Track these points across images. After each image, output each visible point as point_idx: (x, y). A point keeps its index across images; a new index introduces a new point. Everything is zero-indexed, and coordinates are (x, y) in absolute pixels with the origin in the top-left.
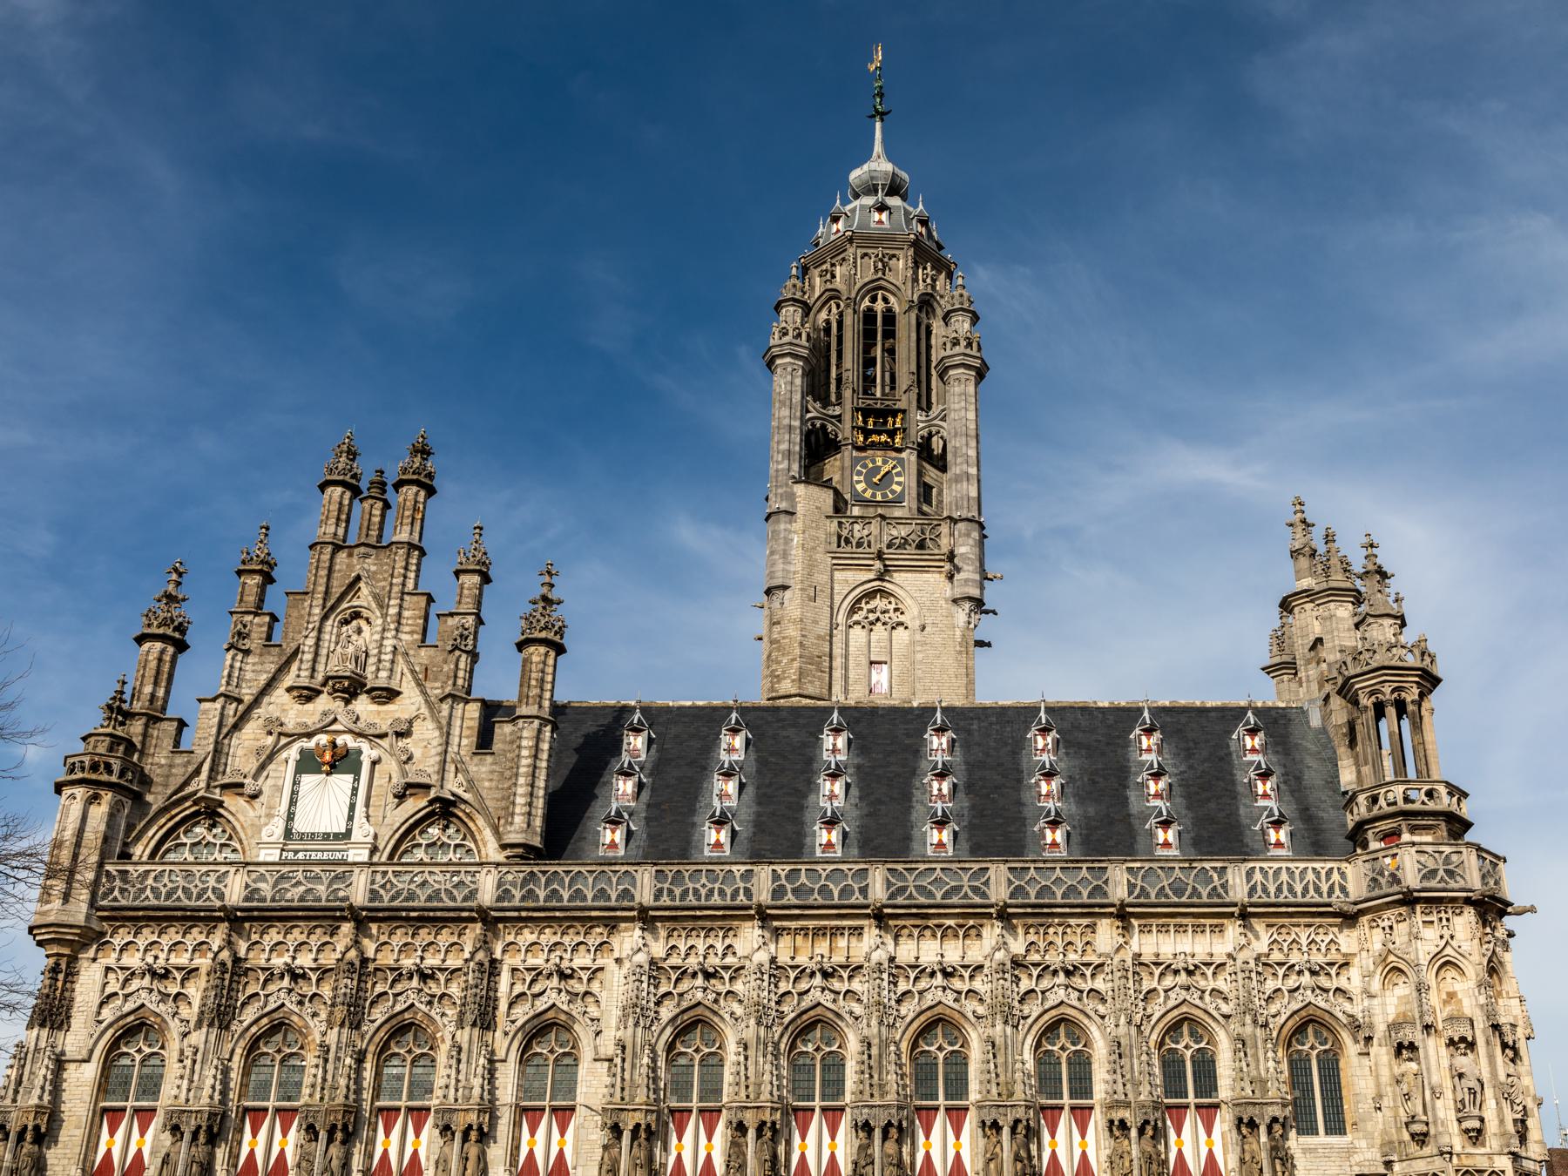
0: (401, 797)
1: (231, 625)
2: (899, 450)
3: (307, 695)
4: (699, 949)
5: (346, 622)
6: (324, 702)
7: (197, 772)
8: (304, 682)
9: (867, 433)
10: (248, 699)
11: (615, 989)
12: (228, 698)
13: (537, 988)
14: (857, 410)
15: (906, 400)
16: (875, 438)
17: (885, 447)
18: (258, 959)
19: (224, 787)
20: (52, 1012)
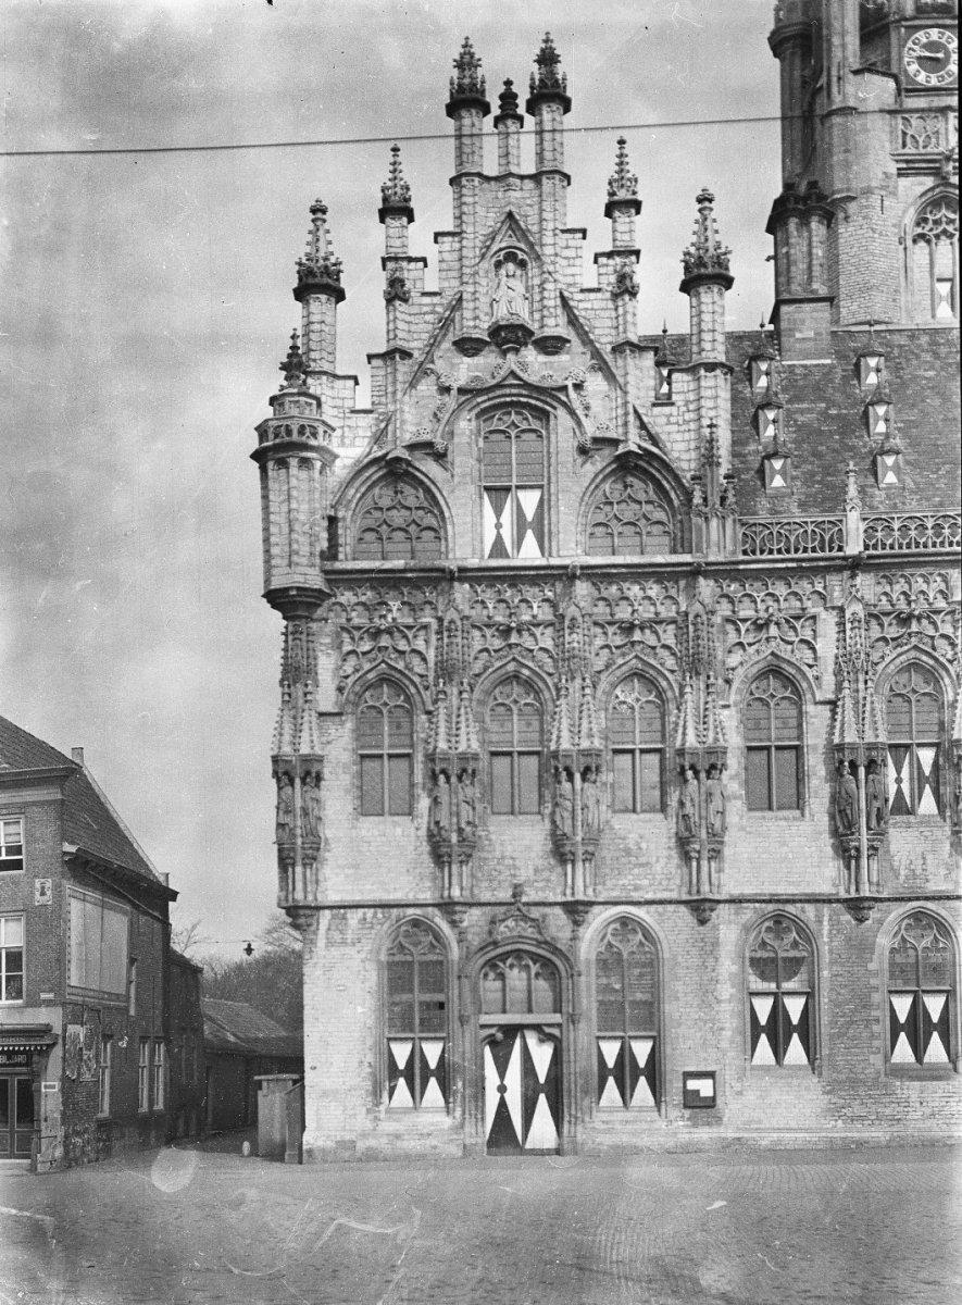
5: (498, 265)
19: (412, 447)
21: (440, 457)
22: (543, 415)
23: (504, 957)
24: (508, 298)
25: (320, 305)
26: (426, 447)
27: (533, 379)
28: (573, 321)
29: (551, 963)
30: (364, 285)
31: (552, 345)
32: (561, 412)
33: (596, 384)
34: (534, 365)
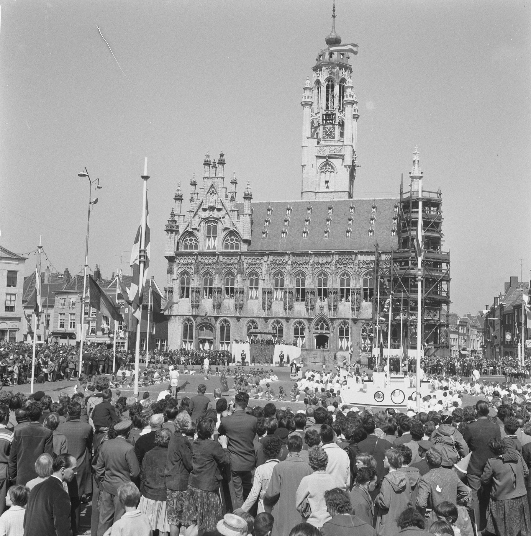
0: (224, 230)
1: (191, 196)
2: (334, 125)
3: (205, 210)
4: (279, 259)
5: (211, 194)
6: (208, 211)
7: (188, 226)
8: (204, 207)
9: (326, 120)
10: (195, 211)
11: (264, 268)
12: (192, 212)
13: (251, 266)
14: (323, 115)
15: (336, 112)
16: (328, 122)
17: (331, 124)
18: (202, 261)
19: (193, 229)
20: (170, 272)
21: (198, 231)
22: (217, 223)
23: (204, 326)
24: (211, 201)
25: (178, 202)
26: (196, 229)
27: (215, 216)
28: (223, 205)
29: (211, 328)
30: (186, 198)
31: (219, 210)
32: (220, 222)
33: (227, 216)
34: (216, 214)
